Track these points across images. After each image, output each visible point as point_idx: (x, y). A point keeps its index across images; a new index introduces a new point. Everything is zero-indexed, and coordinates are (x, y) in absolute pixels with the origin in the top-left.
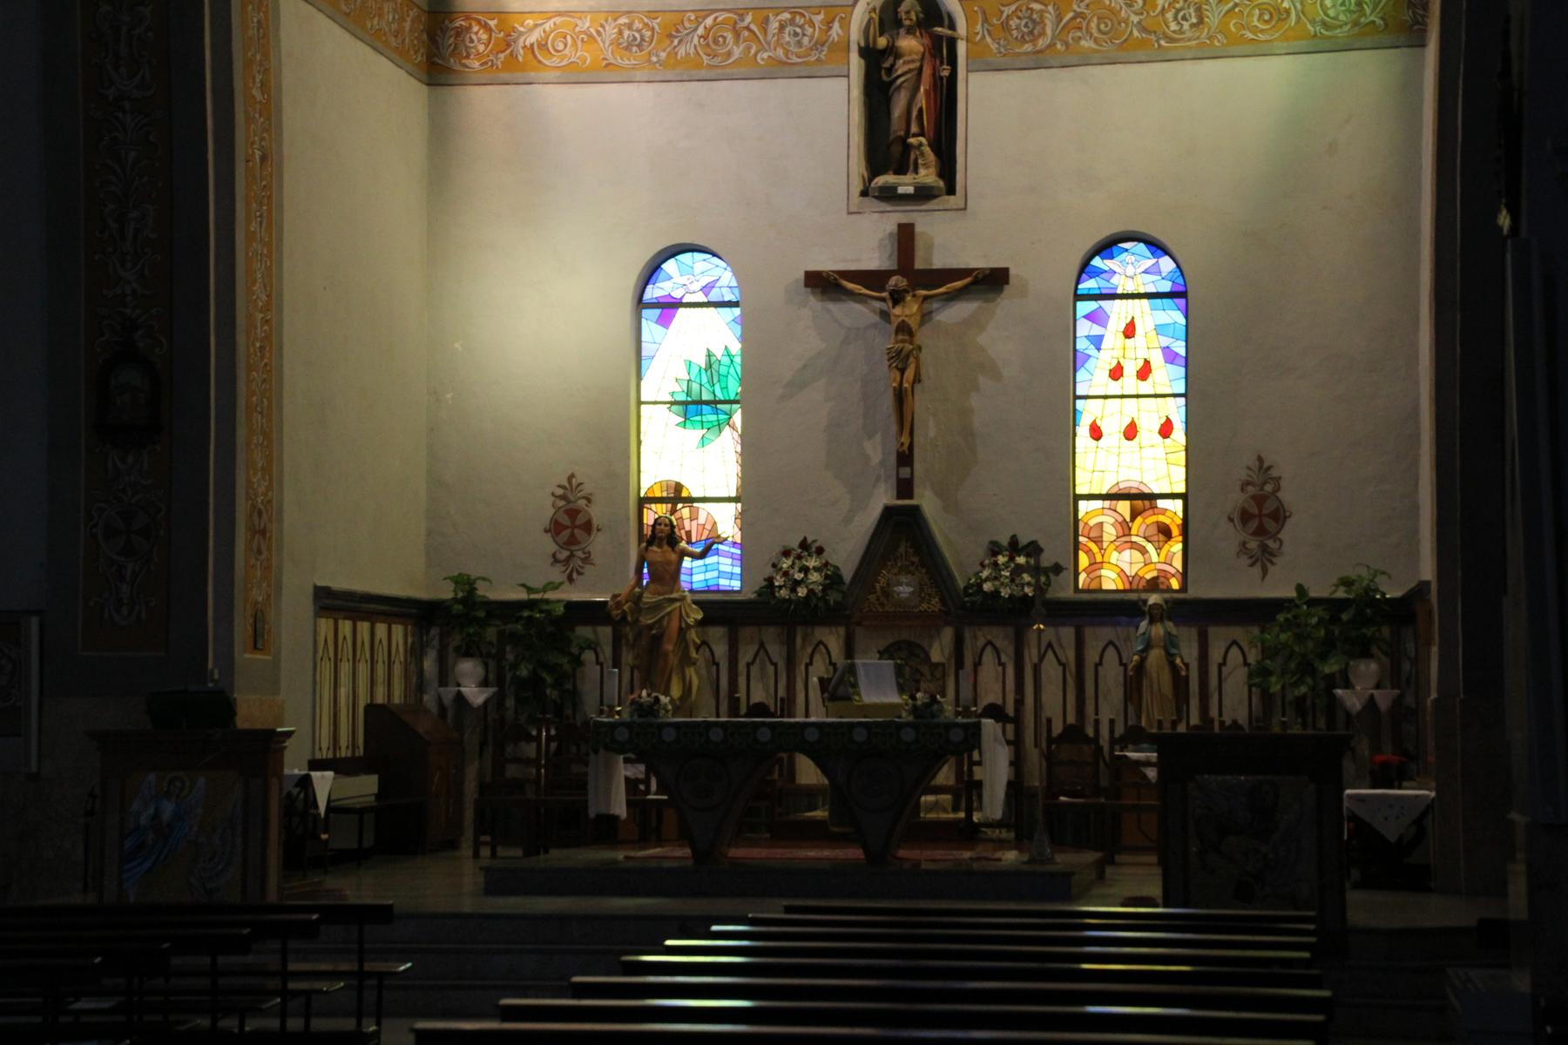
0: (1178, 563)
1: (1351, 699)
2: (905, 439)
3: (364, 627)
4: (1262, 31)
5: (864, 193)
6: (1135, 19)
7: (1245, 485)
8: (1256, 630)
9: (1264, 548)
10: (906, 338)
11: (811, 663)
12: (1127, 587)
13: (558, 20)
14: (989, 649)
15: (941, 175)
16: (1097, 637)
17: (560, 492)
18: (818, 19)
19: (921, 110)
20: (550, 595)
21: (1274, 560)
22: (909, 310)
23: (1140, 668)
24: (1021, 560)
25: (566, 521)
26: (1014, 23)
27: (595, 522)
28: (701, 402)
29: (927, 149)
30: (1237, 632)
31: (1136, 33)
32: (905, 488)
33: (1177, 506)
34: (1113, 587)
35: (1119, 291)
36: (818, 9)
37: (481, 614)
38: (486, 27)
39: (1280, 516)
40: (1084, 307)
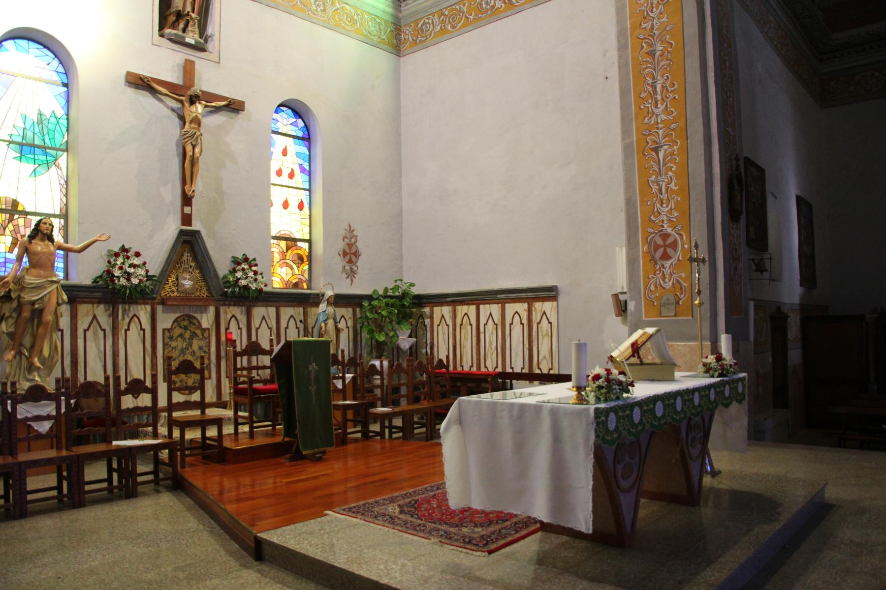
0: (306, 275)
4: (347, 25)
9: (351, 269)
10: (197, 127)
11: (128, 329)
12: (285, 287)
14: (233, 319)
21: (355, 276)
28: (33, 146)
31: (299, 4)
32: (187, 219)
34: (278, 287)
35: (280, 131)
39: (357, 254)
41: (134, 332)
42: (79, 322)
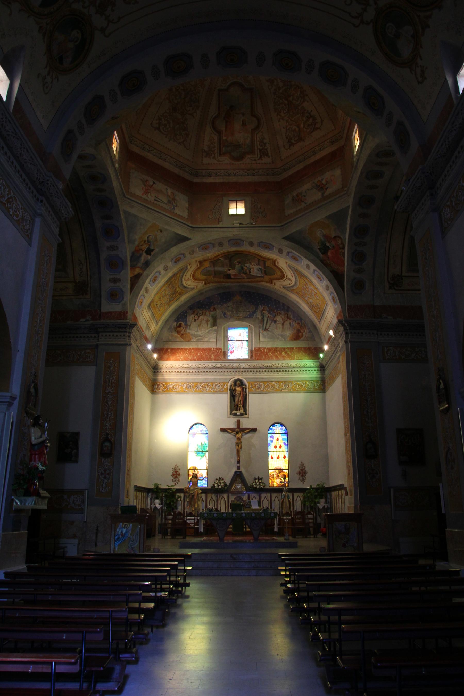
1: (321, 506)
2: (239, 458)
3: (140, 493)
5: (231, 414)
6: (277, 386)
7: (299, 467)
8: (302, 494)
11: (221, 500)
13: (176, 383)
14: (254, 498)
15: (244, 411)
16: (274, 495)
17: (174, 468)
18: (222, 384)
19: (240, 400)
20: (172, 488)
22: (239, 435)
23: (283, 501)
24: (260, 481)
25: (175, 473)
26: (257, 386)
27: (180, 474)
28: (200, 452)
29: (242, 407)
30: (299, 494)
31: (278, 388)
32: (239, 468)
33: (287, 471)
35: (276, 433)
36: (222, 383)
37: (160, 491)
38: (163, 384)
39: (305, 473)
40: (269, 435)
41: (223, 501)
42: (208, 499)
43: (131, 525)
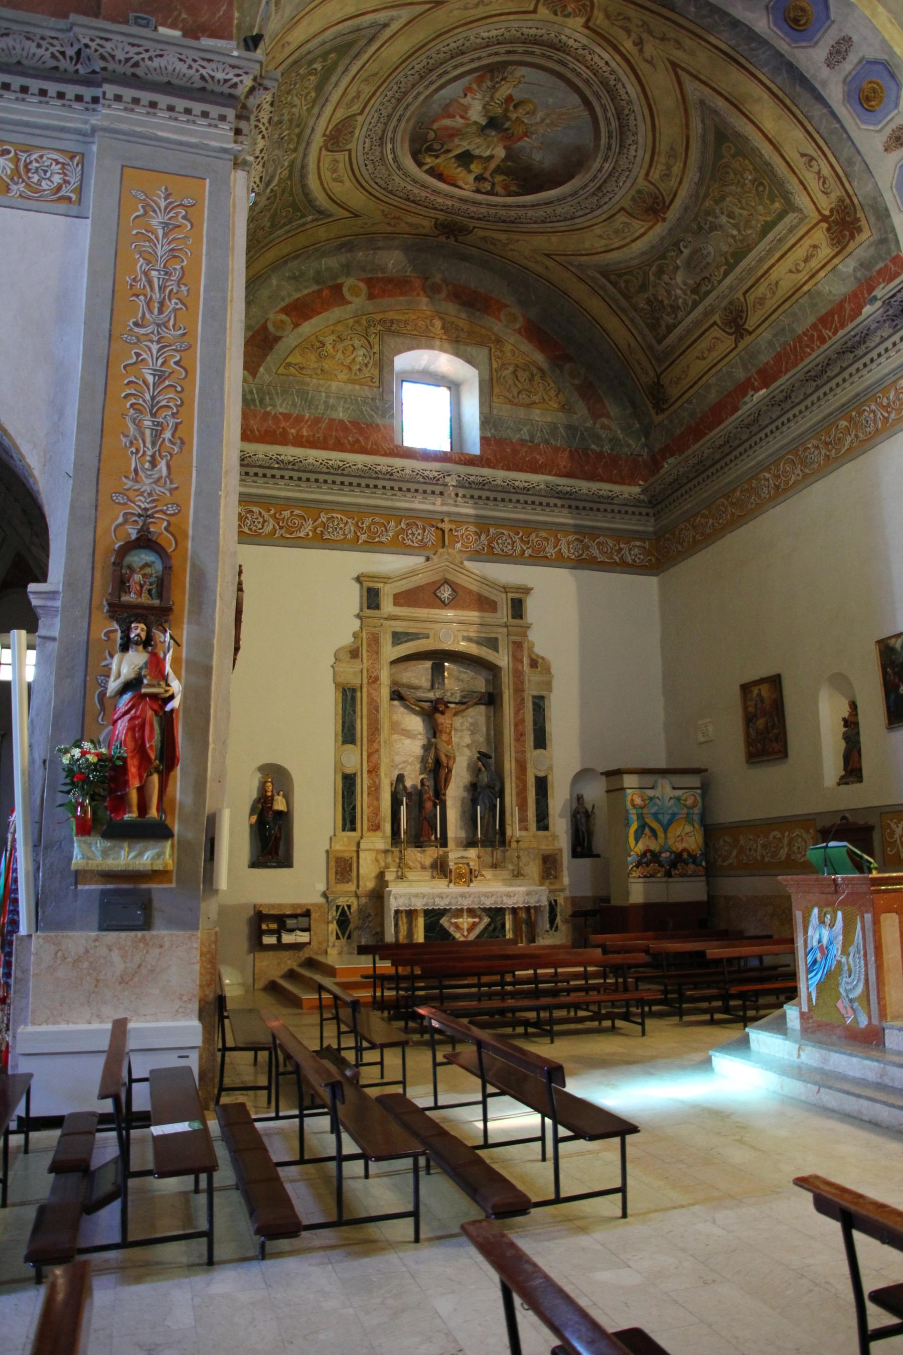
43: (839, 914)
